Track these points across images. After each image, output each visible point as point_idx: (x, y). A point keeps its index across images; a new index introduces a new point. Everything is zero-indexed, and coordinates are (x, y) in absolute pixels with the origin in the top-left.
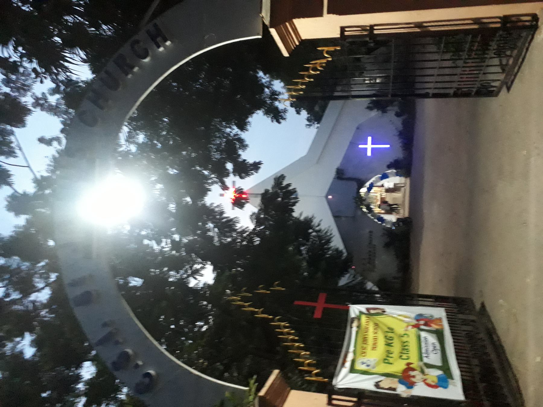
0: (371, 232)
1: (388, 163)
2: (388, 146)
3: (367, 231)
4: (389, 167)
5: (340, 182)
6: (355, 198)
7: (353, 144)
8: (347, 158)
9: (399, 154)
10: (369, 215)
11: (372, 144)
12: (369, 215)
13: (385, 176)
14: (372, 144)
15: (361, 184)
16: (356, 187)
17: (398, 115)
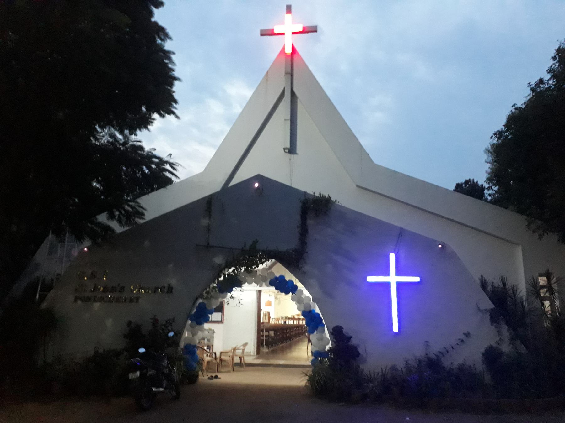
0: (170, 289)
2: (396, 329)
3: (173, 282)
4: (337, 333)
5: (297, 207)
7: (400, 237)
8: (355, 222)
9: (377, 359)
11: (399, 284)
14: (399, 284)
15: (293, 261)
16: (283, 247)
17: (491, 356)
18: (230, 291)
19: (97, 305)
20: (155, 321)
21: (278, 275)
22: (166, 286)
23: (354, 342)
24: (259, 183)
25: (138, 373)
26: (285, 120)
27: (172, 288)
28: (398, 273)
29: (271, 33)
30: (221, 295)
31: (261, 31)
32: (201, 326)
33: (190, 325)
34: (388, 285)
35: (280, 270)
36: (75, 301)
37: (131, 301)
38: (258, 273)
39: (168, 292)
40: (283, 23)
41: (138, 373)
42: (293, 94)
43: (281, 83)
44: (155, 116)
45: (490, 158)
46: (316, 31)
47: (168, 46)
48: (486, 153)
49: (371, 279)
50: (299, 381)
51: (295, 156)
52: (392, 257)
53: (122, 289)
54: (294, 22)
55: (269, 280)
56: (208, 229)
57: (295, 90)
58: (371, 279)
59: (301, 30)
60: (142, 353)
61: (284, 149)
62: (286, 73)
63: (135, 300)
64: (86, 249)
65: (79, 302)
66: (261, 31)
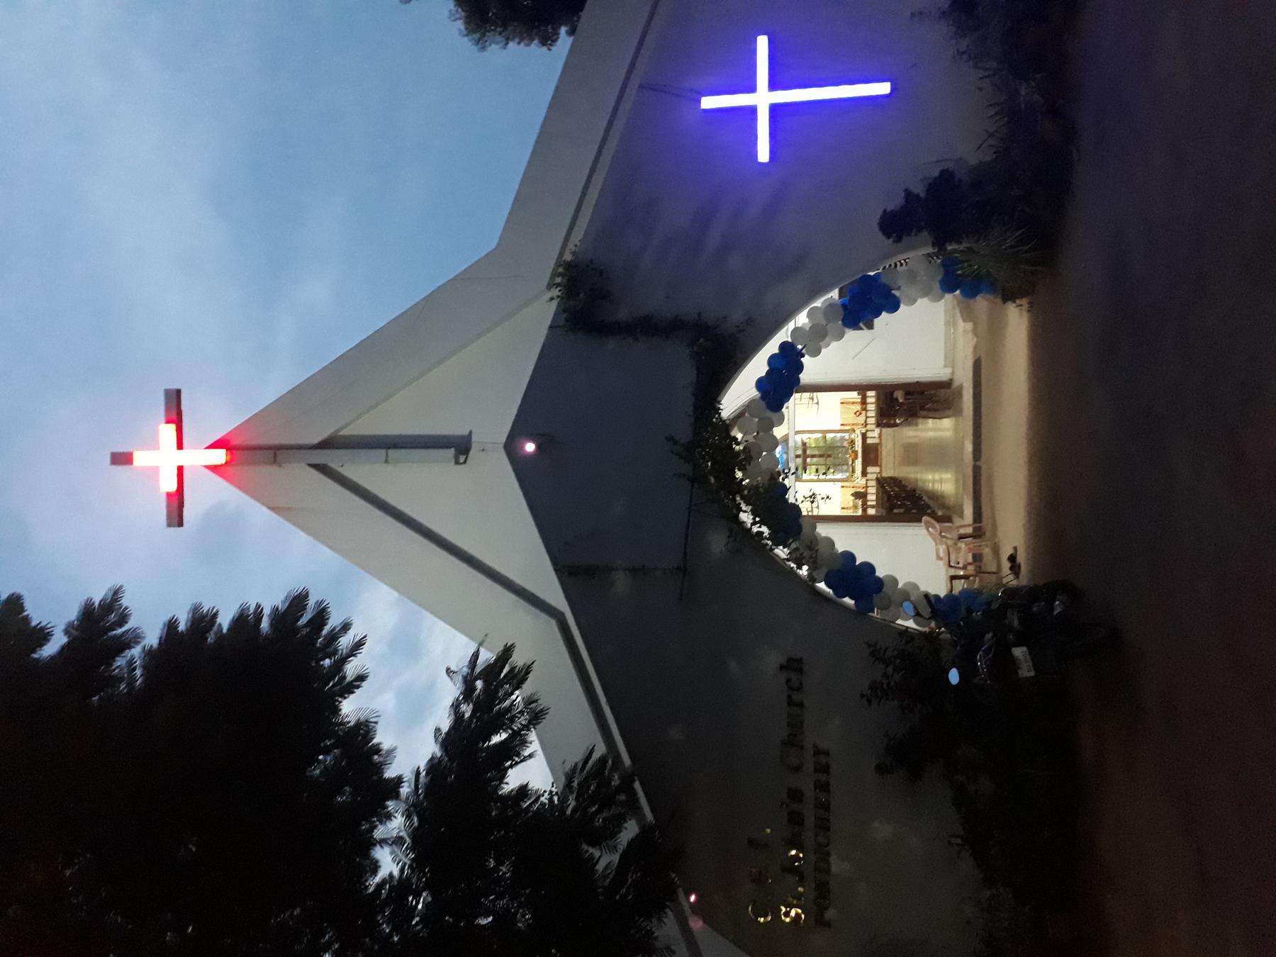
0: (793, 665)
1: (896, 202)
2: (883, 88)
3: (772, 659)
4: (896, 226)
6: (688, 452)
10: (782, 552)
11: (773, 86)
12: (782, 552)
13: (865, 304)
14: (773, 86)
18: (796, 509)
19: (837, 865)
20: (876, 692)
21: (754, 393)
22: (783, 677)
23: (919, 190)
24: (523, 447)
25: (1019, 652)
26: (386, 461)
27: (790, 660)
28: (751, 88)
29: (177, 500)
30: (806, 529)
31: (169, 525)
32: (886, 583)
33: (881, 608)
34: (775, 109)
35: (740, 393)
36: (828, 924)
37: (824, 769)
38: (750, 438)
39: (800, 671)
40: (155, 471)
41: (1019, 652)
42: (326, 444)
43: (299, 476)
44: (350, 708)
45: (499, 38)
46: (179, 392)
47: (148, 622)
48: (483, 48)
49: (763, 155)
50: (1017, 323)
51: (474, 439)
52: (708, 103)
53: (796, 795)
54: (153, 444)
55: (769, 414)
56: (637, 572)
57: (315, 441)
58: (763, 155)
59: (173, 427)
60: (960, 674)
61: (457, 462)
62: (274, 461)
63: (823, 759)
64: (693, 898)
65: (830, 914)
66: (169, 525)
